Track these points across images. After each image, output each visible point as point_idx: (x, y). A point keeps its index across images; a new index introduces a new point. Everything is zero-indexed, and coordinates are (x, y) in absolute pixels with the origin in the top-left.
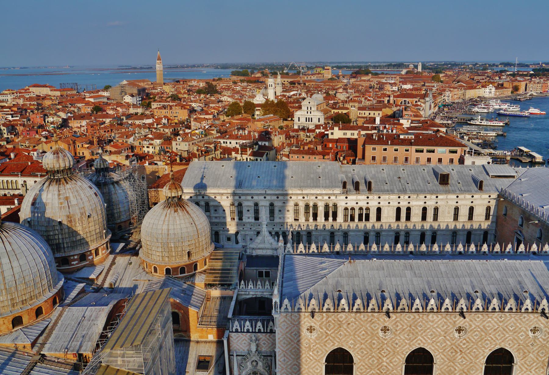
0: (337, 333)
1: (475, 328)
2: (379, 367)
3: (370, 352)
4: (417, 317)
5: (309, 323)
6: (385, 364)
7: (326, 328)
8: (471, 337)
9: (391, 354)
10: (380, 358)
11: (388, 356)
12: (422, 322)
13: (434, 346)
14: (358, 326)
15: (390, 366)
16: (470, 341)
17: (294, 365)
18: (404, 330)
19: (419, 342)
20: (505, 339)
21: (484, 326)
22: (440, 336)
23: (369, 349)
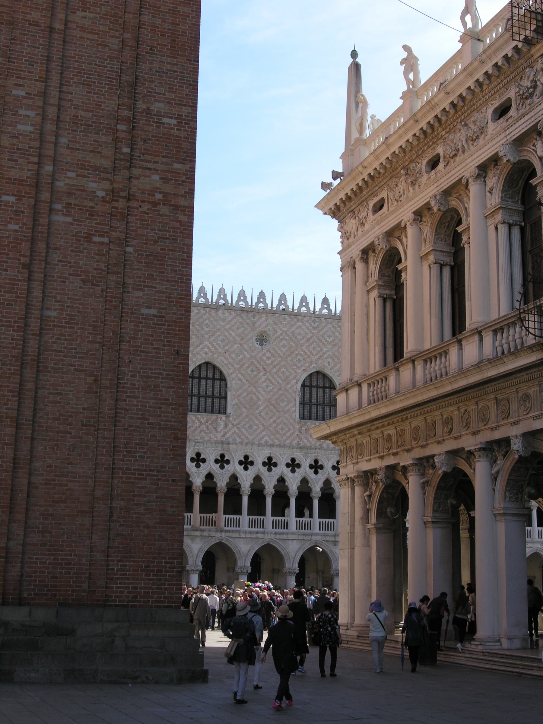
1: (281, 335)
4: (203, 312)
8: (277, 349)
12: (209, 320)
13: (227, 359)
16: (276, 355)
20: (323, 355)
21: (293, 333)
22: (236, 344)
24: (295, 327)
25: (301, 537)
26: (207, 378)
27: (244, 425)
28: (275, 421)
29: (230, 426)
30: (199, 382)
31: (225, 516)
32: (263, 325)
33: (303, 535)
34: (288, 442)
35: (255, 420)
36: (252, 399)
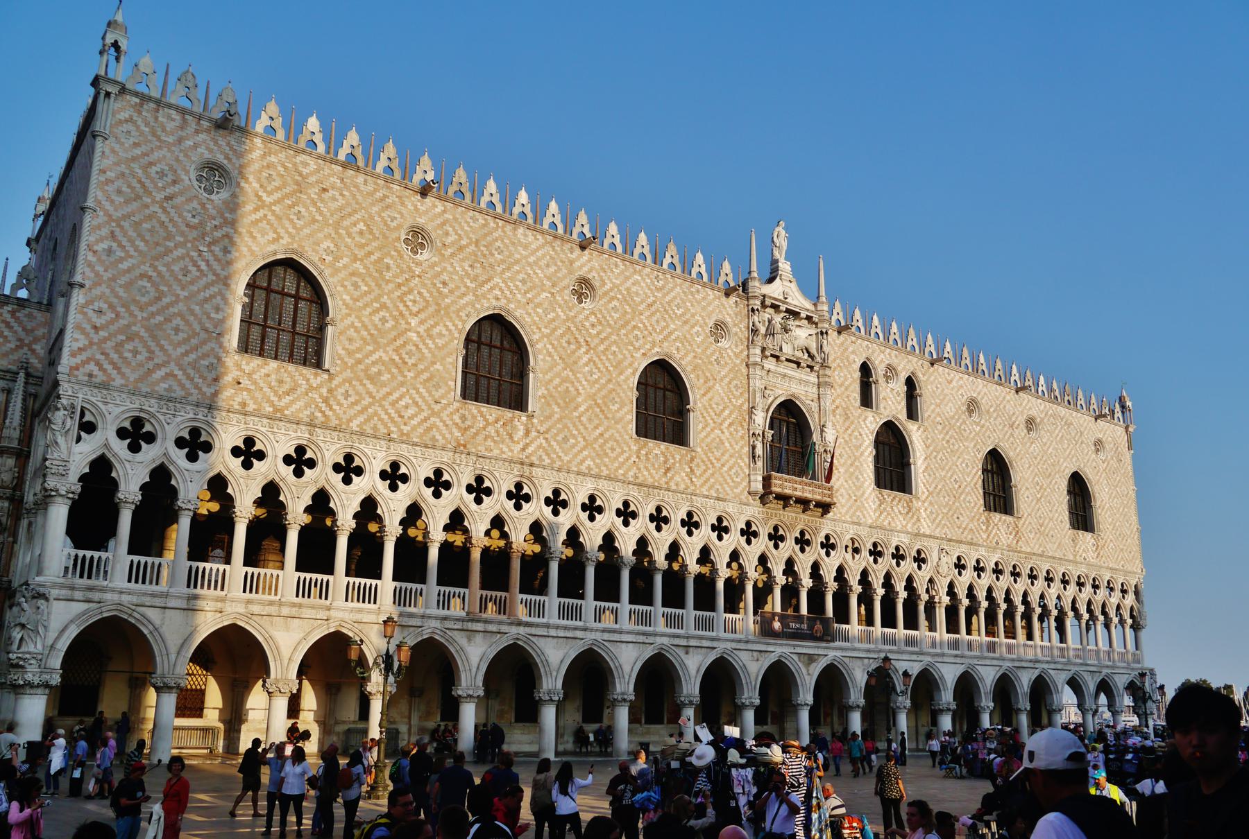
0: (290, 207)
1: (611, 289)
2: (399, 342)
3: (377, 291)
4: (492, 225)
5: (211, 151)
6: (413, 336)
7: (259, 180)
9: (432, 309)
10: (401, 314)
11: (422, 316)
14: (348, 204)
15: (424, 344)
17: (142, 276)
18: (461, 249)
19: (497, 292)
21: (628, 289)
23: (374, 279)
24: (631, 281)
25: (641, 639)
26: (491, 346)
27: (556, 435)
28: (601, 435)
29: (534, 434)
30: (479, 348)
31: (521, 596)
32: (585, 269)
33: (644, 634)
34: (621, 471)
35: (570, 425)
36: (567, 390)
